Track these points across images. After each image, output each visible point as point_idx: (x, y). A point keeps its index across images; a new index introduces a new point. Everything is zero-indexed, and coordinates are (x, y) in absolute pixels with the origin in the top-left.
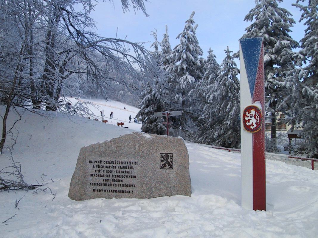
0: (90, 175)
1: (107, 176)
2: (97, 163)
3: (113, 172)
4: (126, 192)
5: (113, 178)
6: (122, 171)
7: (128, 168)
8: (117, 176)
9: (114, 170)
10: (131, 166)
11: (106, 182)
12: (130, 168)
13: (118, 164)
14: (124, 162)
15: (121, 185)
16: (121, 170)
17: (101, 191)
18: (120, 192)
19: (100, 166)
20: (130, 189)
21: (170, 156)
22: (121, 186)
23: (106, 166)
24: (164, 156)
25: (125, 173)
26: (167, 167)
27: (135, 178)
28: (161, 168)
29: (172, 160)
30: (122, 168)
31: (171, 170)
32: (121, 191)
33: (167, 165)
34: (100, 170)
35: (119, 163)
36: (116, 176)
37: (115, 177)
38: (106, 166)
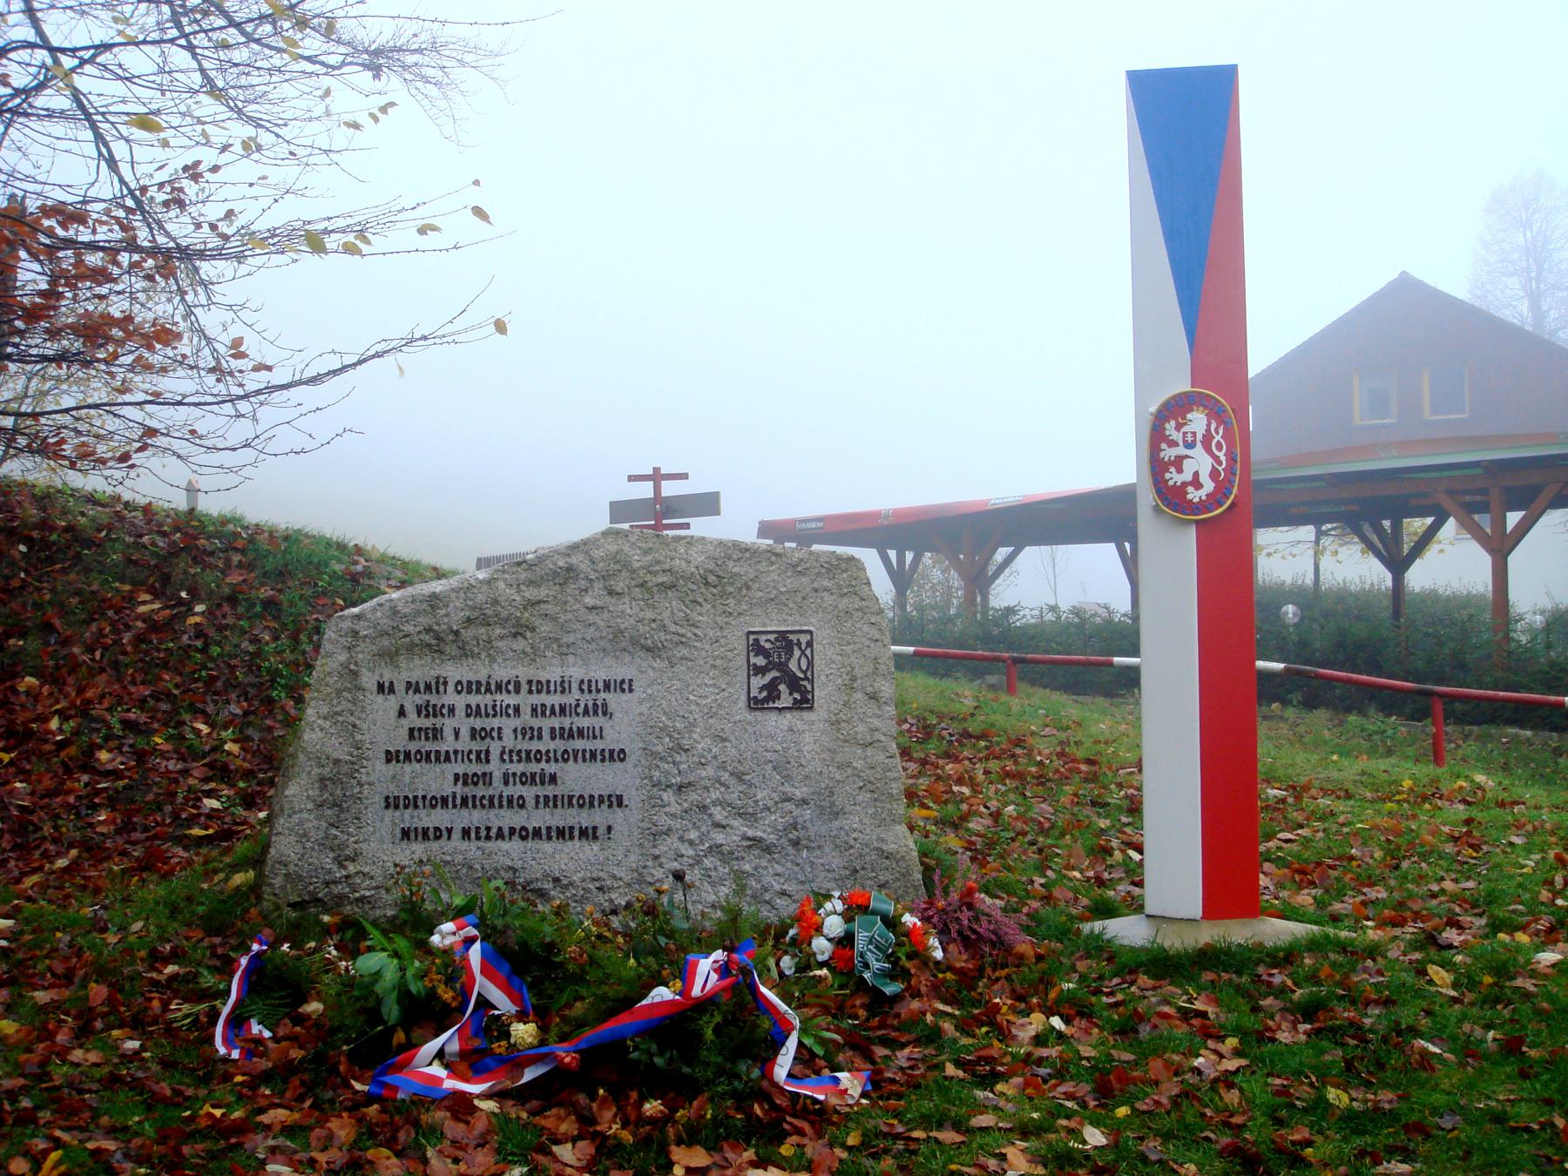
0: (383, 756)
1: (473, 757)
2: (417, 690)
3: (508, 734)
4: (576, 833)
5: (508, 766)
6: (553, 729)
7: (586, 712)
8: (528, 753)
9: (508, 724)
10: (599, 703)
11: (469, 791)
12: (596, 713)
13: (530, 692)
14: (563, 682)
15: (546, 797)
16: (546, 723)
17: (445, 833)
18: (544, 837)
19: (435, 706)
20: (598, 817)
21: (799, 644)
22: (546, 804)
23: (468, 706)
24: (768, 646)
25: (571, 736)
26: (786, 700)
27: (622, 760)
28: (755, 704)
29: (810, 664)
30: (553, 712)
31: (806, 715)
32: (549, 829)
33: (782, 687)
34: (435, 729)
35: (534, 688)
36: (523, 755)
37: (515, 758)
38: (468, 706)
